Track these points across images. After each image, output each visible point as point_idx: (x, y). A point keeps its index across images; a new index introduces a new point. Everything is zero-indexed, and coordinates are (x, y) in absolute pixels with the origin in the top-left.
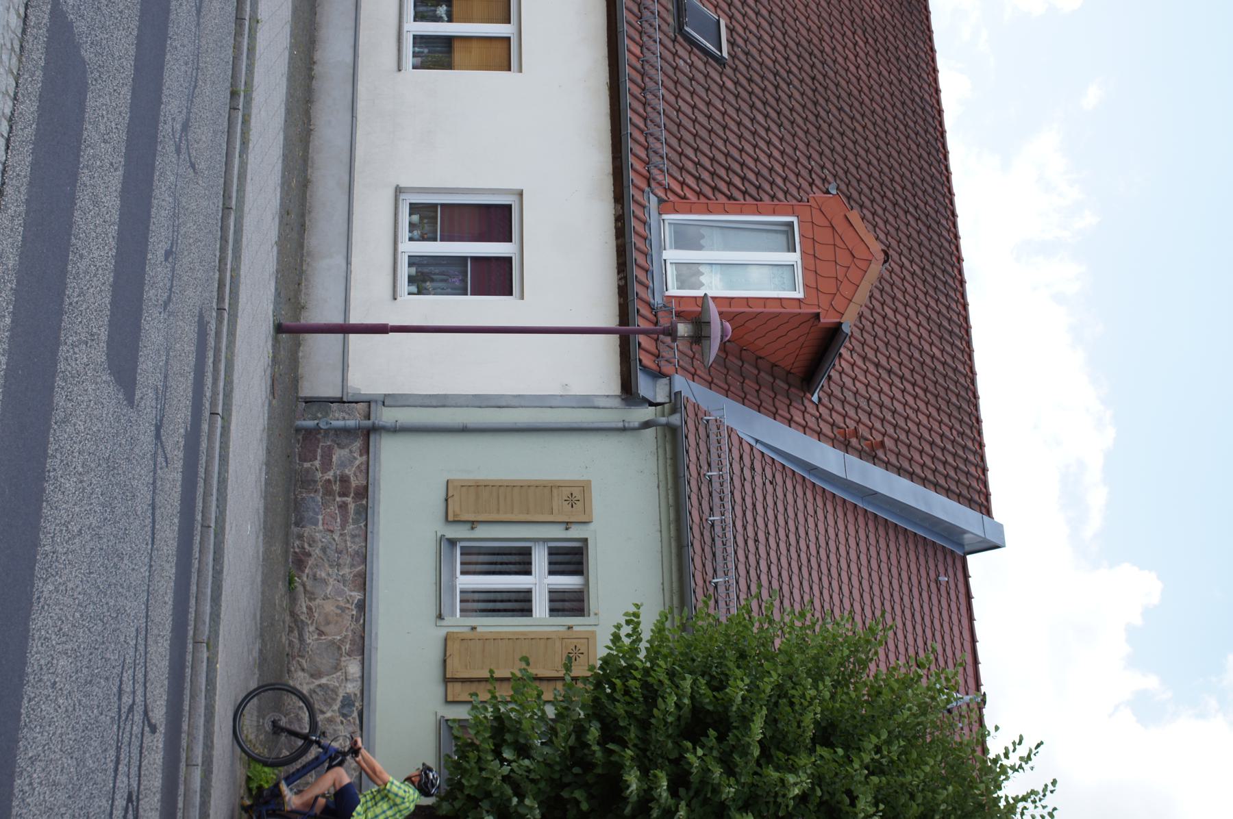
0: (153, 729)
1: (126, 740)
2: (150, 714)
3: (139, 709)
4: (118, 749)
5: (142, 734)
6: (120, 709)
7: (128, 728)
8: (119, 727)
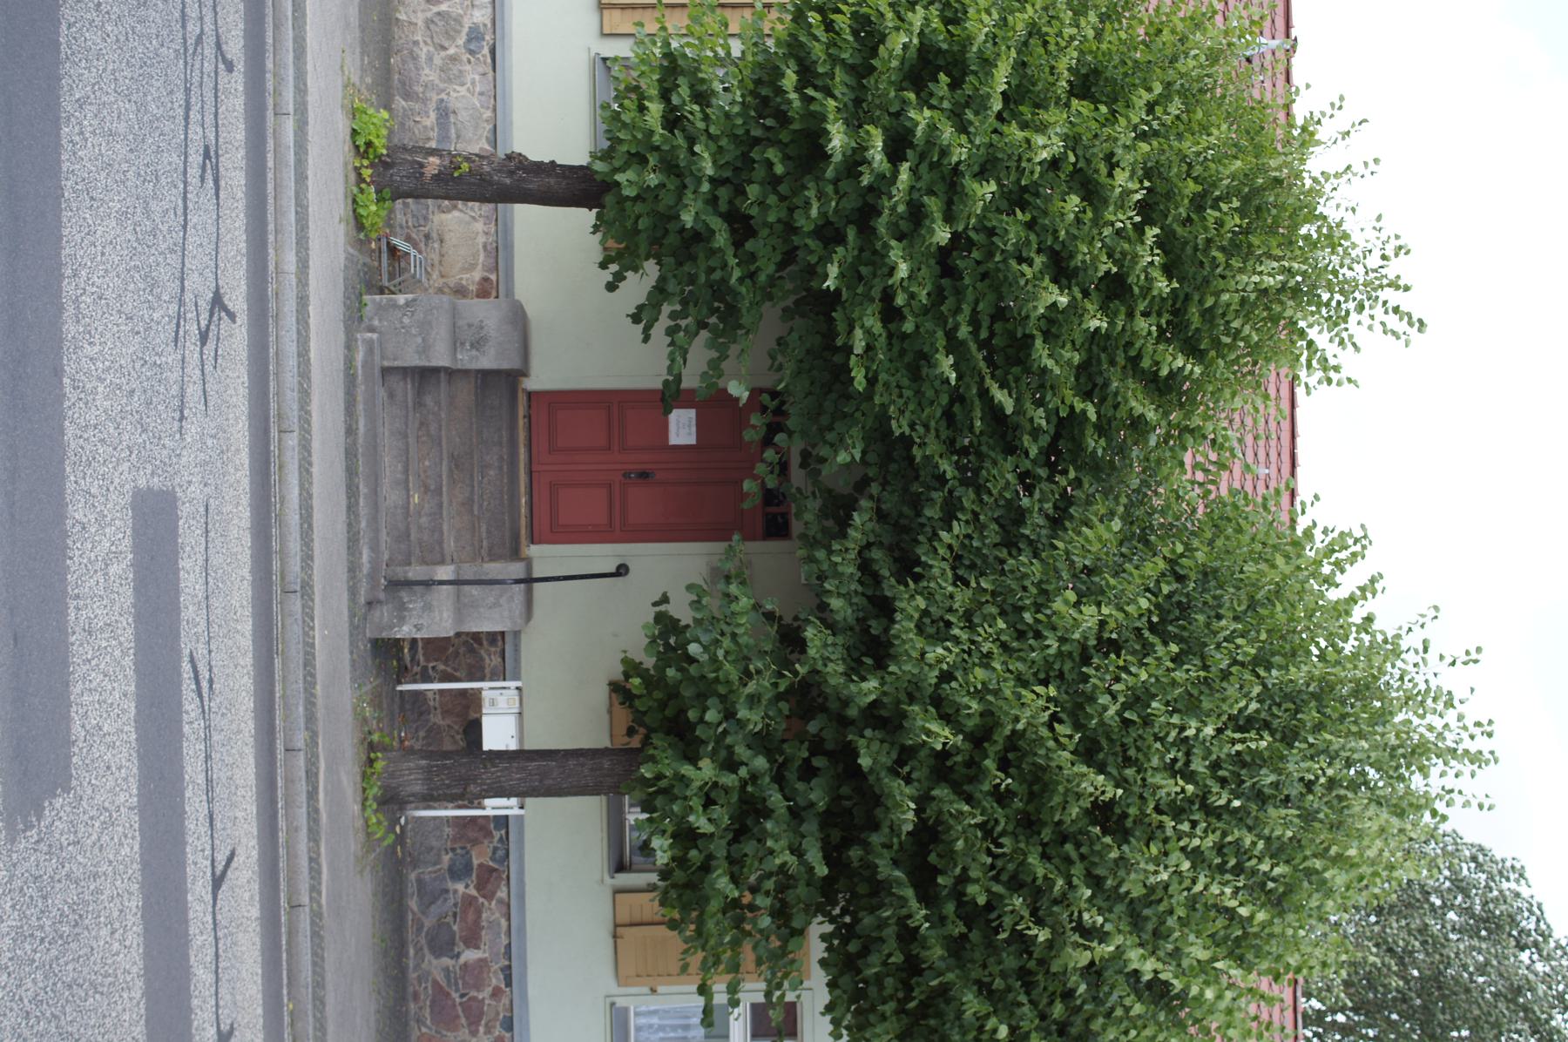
0: (230, 67)
1: (196, 79)
2: (224, 47)
3: (209, 41)
4: (187, 91)
5: (216, 73)
6: (185, 39)
7: (197, 66)
8: (186, 63)
